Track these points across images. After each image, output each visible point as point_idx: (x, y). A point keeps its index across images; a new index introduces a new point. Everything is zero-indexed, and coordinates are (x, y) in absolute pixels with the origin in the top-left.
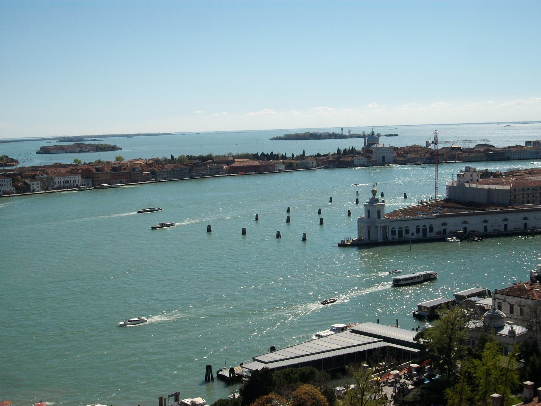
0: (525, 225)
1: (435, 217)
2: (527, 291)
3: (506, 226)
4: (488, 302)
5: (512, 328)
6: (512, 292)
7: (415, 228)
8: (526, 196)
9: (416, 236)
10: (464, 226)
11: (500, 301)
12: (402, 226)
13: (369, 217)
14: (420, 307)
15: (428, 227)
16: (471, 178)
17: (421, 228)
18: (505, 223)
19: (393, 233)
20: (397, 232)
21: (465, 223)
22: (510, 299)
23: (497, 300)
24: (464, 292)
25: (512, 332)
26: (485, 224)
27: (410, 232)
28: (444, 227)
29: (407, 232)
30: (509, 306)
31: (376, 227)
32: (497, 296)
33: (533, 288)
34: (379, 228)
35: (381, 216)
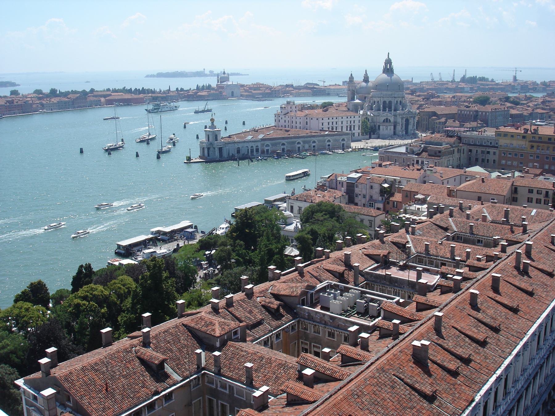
1: (260, 140)
2: (311, 197)
4: (285, 205)
5: (296, 225)
6: (301, 197)
8: (331, 124)
10: (282, 147)
11: (292, 205)
13: (209, 140)
14: (236, 210)
16: (291, 110)
17: (250, 148)
24: (271, 198)
25: (296, 227)
31: (214, 148)
32: (290, 201)
34: (216, 149)
35: (218, 140)
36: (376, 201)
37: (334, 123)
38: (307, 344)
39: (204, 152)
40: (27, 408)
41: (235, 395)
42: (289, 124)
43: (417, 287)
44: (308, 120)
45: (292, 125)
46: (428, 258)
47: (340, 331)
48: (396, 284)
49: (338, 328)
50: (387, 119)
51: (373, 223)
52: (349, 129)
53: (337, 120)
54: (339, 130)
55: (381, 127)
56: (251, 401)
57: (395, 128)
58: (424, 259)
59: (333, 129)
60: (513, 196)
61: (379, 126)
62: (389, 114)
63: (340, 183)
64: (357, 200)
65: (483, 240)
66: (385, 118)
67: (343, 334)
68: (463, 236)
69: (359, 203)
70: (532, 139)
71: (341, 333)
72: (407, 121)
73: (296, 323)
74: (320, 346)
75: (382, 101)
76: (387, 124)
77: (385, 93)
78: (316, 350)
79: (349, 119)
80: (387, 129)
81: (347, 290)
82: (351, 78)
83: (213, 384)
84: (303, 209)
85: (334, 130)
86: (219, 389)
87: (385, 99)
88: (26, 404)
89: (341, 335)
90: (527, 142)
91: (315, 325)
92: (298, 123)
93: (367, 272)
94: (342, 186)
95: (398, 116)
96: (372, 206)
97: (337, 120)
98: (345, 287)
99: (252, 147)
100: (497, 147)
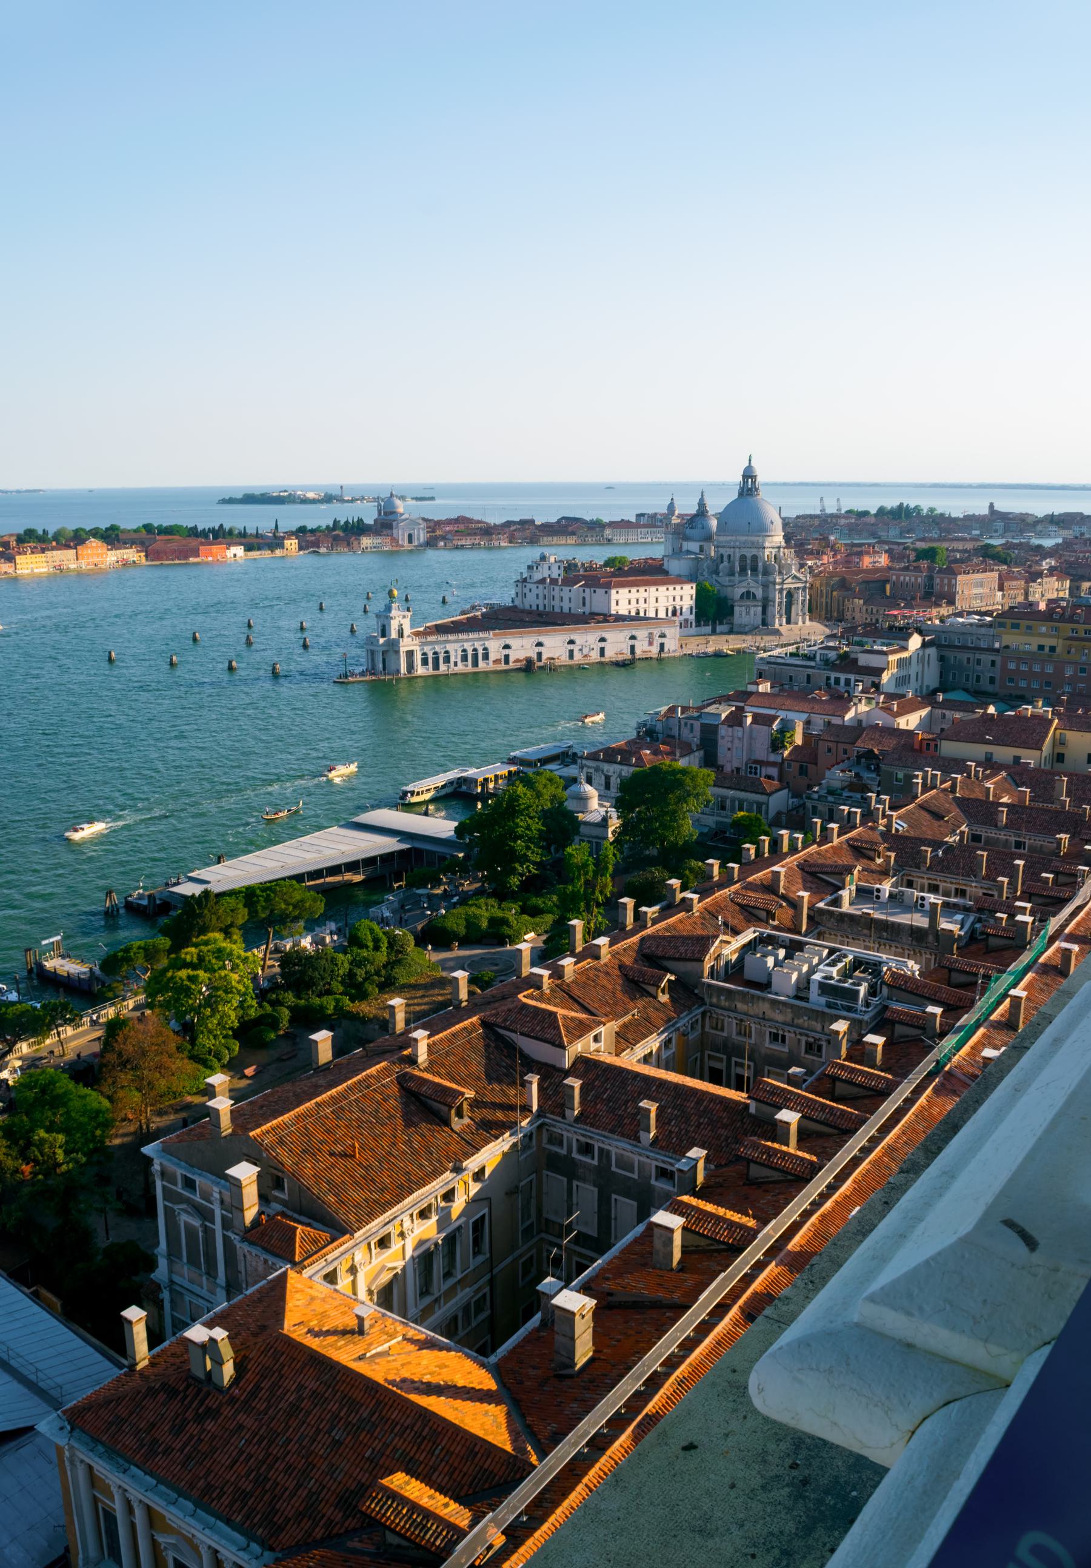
0: (633, 648)
3: (602, 650)
7: (460, 653)
8: (634, 602)
9: (461, 668)
11: (590, 770)
12: (437, 649)
15: (480, 652)
16: (550, 572)
17: (470, 653)
18: (602, 644)
19: (425, 662)
20: (430, 661)
21: (539, 644)
22: (606, 767)
23: (585, 769)
26: (571, 647)
27: (452, 659)
28: (507, 652)
29: (447, 660)
30: (603, 777)
32: (584, 762)
33: (642, 748)
36: (762, 763)
37: (642, 601)
38: (720, 1060)
39: (373, 660)
40: (165, 1207)
41: (614, 1168)
42: (546, 602)
43: (931, 938)
44: (587, 594)
45: (553, 603)
46: (929, 879)
47: (798, 1031)
48: (885, 934)
49: (792, 1026)
50: (748, 592)
51: (764, 807)
52: (670, 614)
53: (646, 595)
54: (652, 614)
55: (737, 609)
56: (650, 1178)
57: (764, 612)
58: (920, 880)
59: (638, 613)
60: (1057, 751)
61: (732, 607)
62: (752, 584)
63: (686, 724)
64: (720, 761)
65: (1027, 841)
66: (744, 590)
67: (804, 1039)
68: (984, 835)
69: (728, 769)
70: (1071, 634)
71: (799, 1037)
72: (790, 595)
73: (699, 1017)
74: (752, 1064)
75: (738, 555)
76: (748, 603)
77: (743, 538)
78: (739, 1071)
79: (671, 592)
80: (748, 613)
81: (799, 946)
82: (671, 507)
83: (561, 1144)
84: (613, 780)
85: (642, 614)
86: (575, 1155)
87: (744, 551)
88: (165, 1199)
89: (799, 1040)
90: (1060, 641)
91: (742, 1020)
92: (566, 599)
93: (821, 911)
94: (692, 730)
95: (771, 586)
96: (756, 773)
97: (646, 595)
98: (791, 940)
99: (475, 650)
100: (998, 651)
